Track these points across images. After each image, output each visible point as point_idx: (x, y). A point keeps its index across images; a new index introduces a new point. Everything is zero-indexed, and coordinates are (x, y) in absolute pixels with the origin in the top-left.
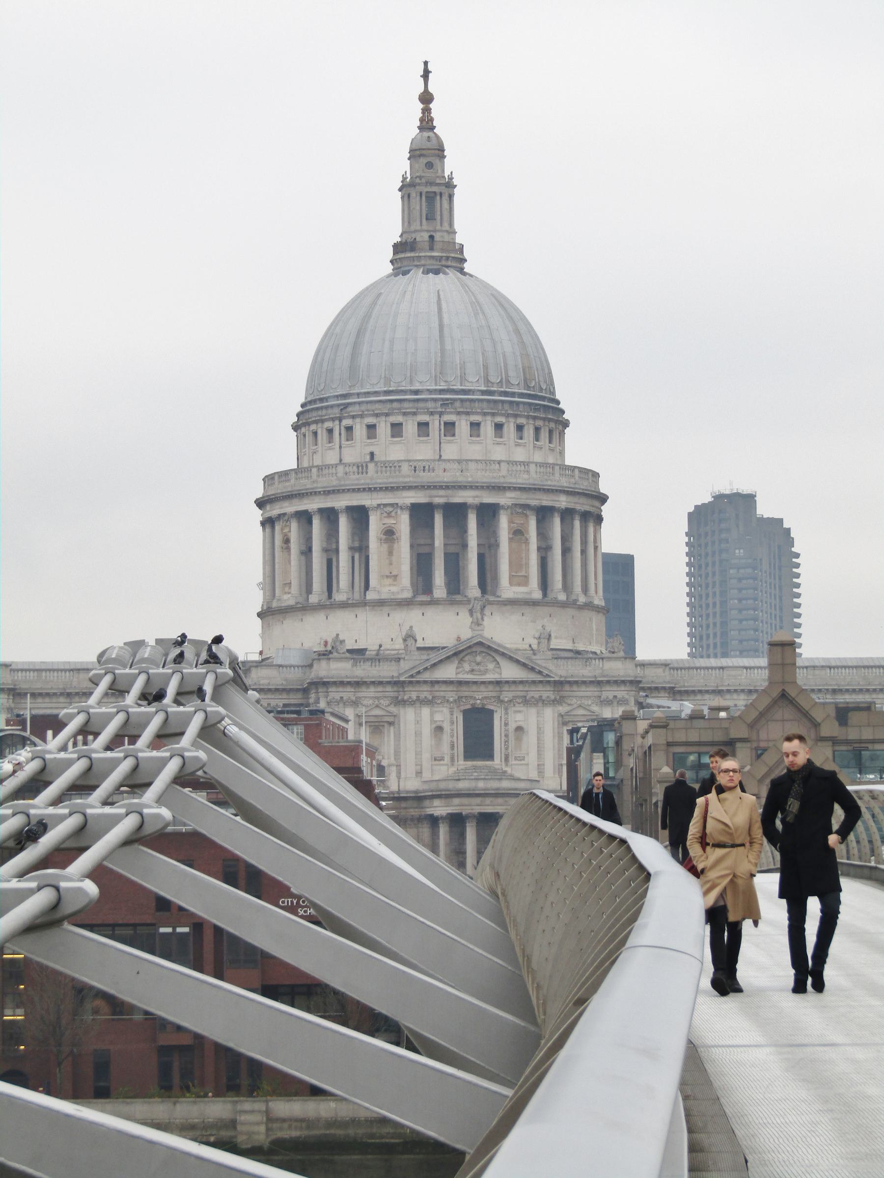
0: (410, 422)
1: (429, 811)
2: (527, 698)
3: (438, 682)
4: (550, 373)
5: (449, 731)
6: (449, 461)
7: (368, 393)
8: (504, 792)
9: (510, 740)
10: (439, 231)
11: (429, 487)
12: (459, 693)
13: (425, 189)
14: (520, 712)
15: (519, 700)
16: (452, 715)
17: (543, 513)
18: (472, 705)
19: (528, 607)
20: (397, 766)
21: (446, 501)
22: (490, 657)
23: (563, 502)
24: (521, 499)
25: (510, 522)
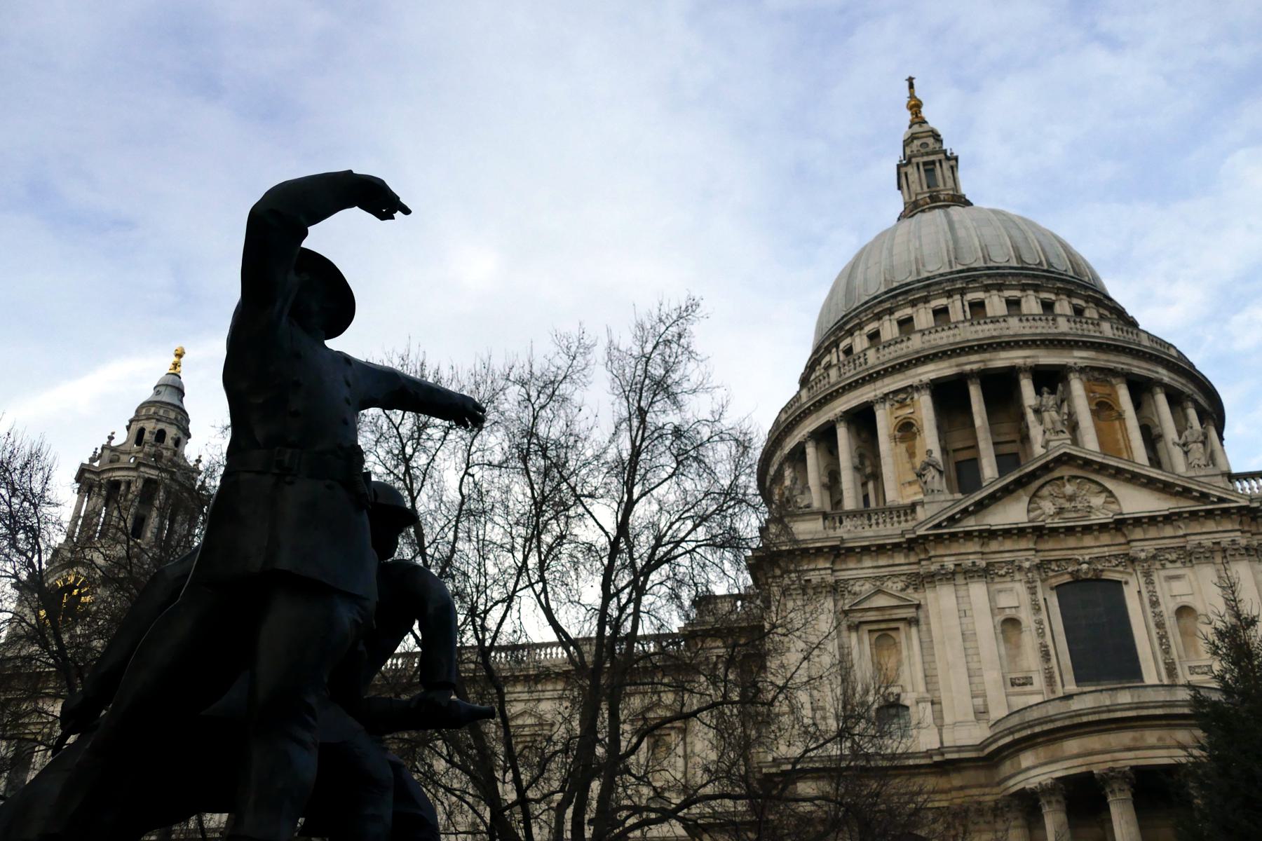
1: (1016, 784)
2: (1188, 548)
3: (991, 534)
5: (1034, 626)
7: (866, 303)
10: (942, 190)
11: (953, 351)
12: (1041, 554)
14: (1177, 577)
15: (1174, 556)
16: (1034, 593)
20: (933, 703)
21: (982, 368)
22: (1091, 485)
23: (1164, 375)
24: (1100, 360)
25: (1088, 390)
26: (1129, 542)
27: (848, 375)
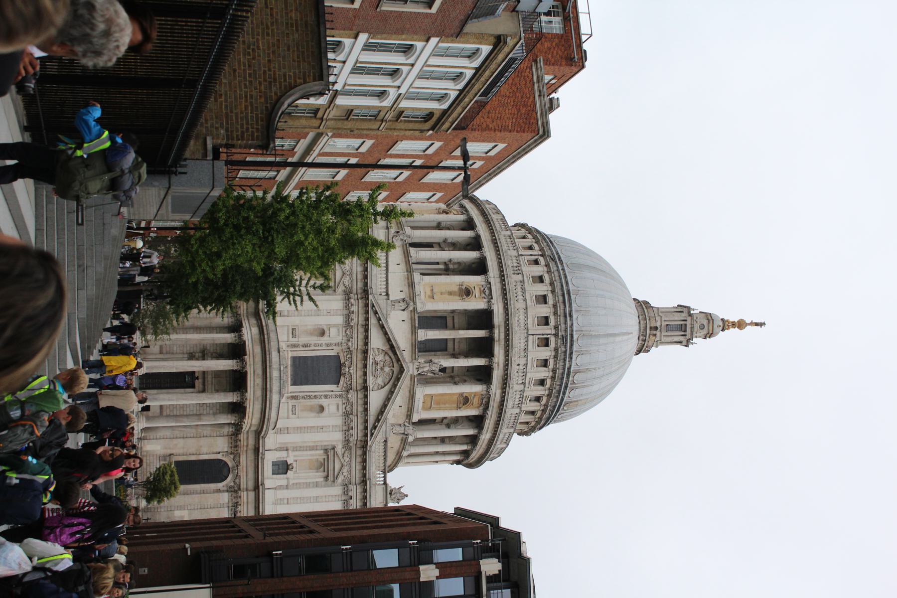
0: (548, 310)
1: (245, 324)
2: (351, 416)
3: (366, 331)
4: (563, 420)
5: (320, 342)
6: (527, 341)
7: (566, 277)
8: (268, 396)
9: (312, 400)
11: (508, 325)
12: (356, 351)
13: (688, 323)
14: (338, 409)
15: (348, 409)
17: (478, 421)
18: (344, 363)
19: (406, 411)
23: (485, 436)
25: (475, 394)
26: (357, 391)
27: (509, 263)
